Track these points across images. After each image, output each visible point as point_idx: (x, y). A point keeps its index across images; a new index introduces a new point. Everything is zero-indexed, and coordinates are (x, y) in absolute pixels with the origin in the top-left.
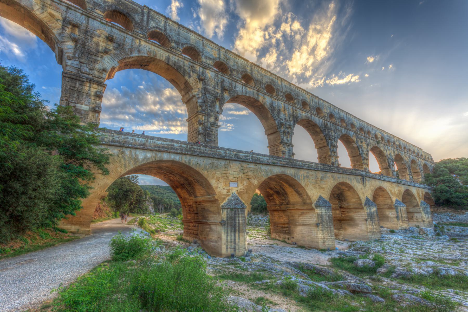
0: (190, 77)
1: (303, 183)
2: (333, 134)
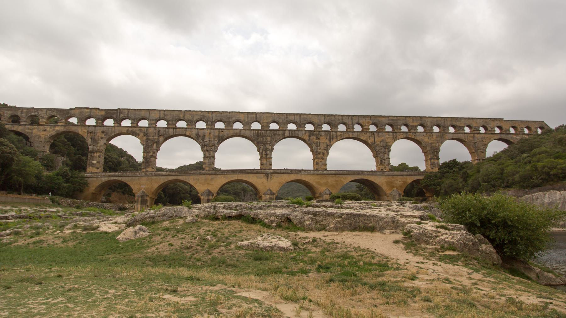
0: (139, 135)
1: (192, 183)
2: (269, 139)
